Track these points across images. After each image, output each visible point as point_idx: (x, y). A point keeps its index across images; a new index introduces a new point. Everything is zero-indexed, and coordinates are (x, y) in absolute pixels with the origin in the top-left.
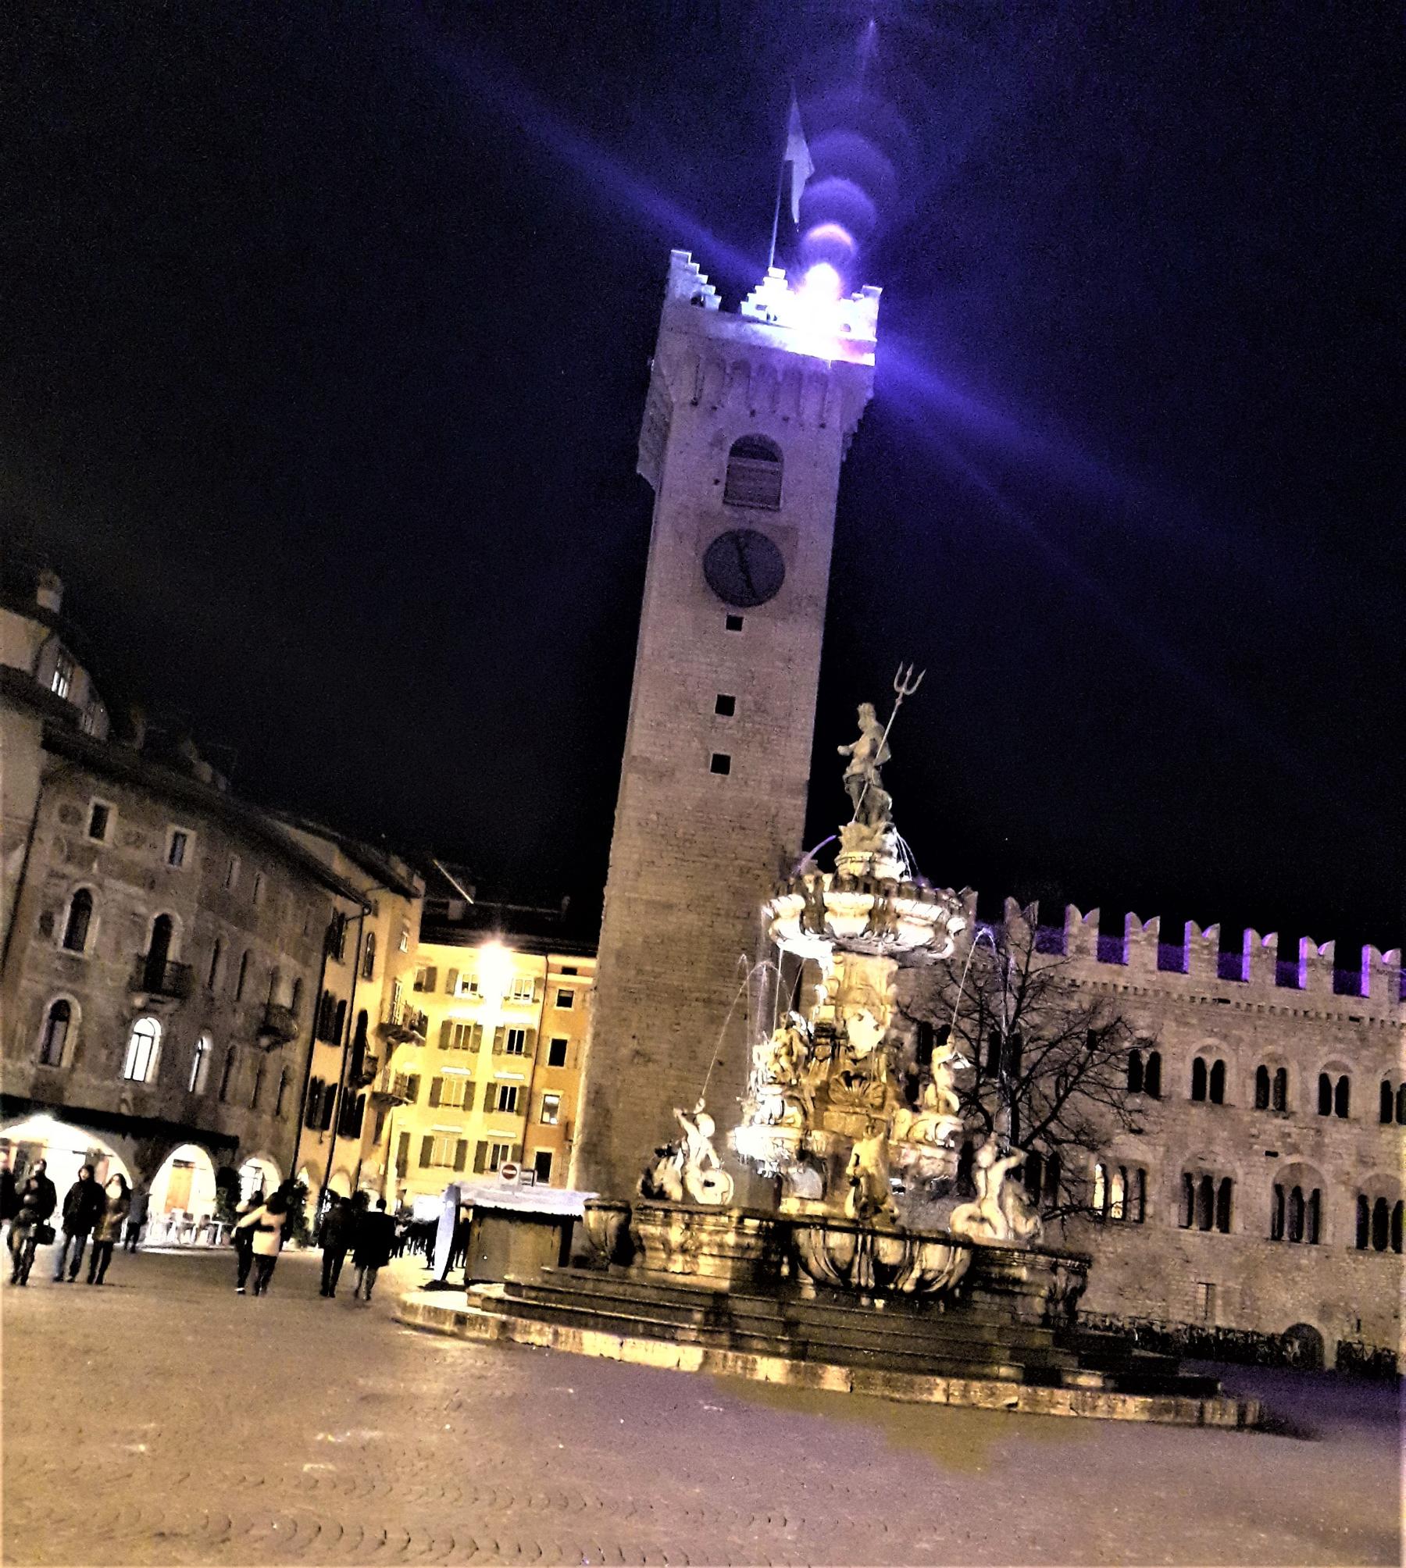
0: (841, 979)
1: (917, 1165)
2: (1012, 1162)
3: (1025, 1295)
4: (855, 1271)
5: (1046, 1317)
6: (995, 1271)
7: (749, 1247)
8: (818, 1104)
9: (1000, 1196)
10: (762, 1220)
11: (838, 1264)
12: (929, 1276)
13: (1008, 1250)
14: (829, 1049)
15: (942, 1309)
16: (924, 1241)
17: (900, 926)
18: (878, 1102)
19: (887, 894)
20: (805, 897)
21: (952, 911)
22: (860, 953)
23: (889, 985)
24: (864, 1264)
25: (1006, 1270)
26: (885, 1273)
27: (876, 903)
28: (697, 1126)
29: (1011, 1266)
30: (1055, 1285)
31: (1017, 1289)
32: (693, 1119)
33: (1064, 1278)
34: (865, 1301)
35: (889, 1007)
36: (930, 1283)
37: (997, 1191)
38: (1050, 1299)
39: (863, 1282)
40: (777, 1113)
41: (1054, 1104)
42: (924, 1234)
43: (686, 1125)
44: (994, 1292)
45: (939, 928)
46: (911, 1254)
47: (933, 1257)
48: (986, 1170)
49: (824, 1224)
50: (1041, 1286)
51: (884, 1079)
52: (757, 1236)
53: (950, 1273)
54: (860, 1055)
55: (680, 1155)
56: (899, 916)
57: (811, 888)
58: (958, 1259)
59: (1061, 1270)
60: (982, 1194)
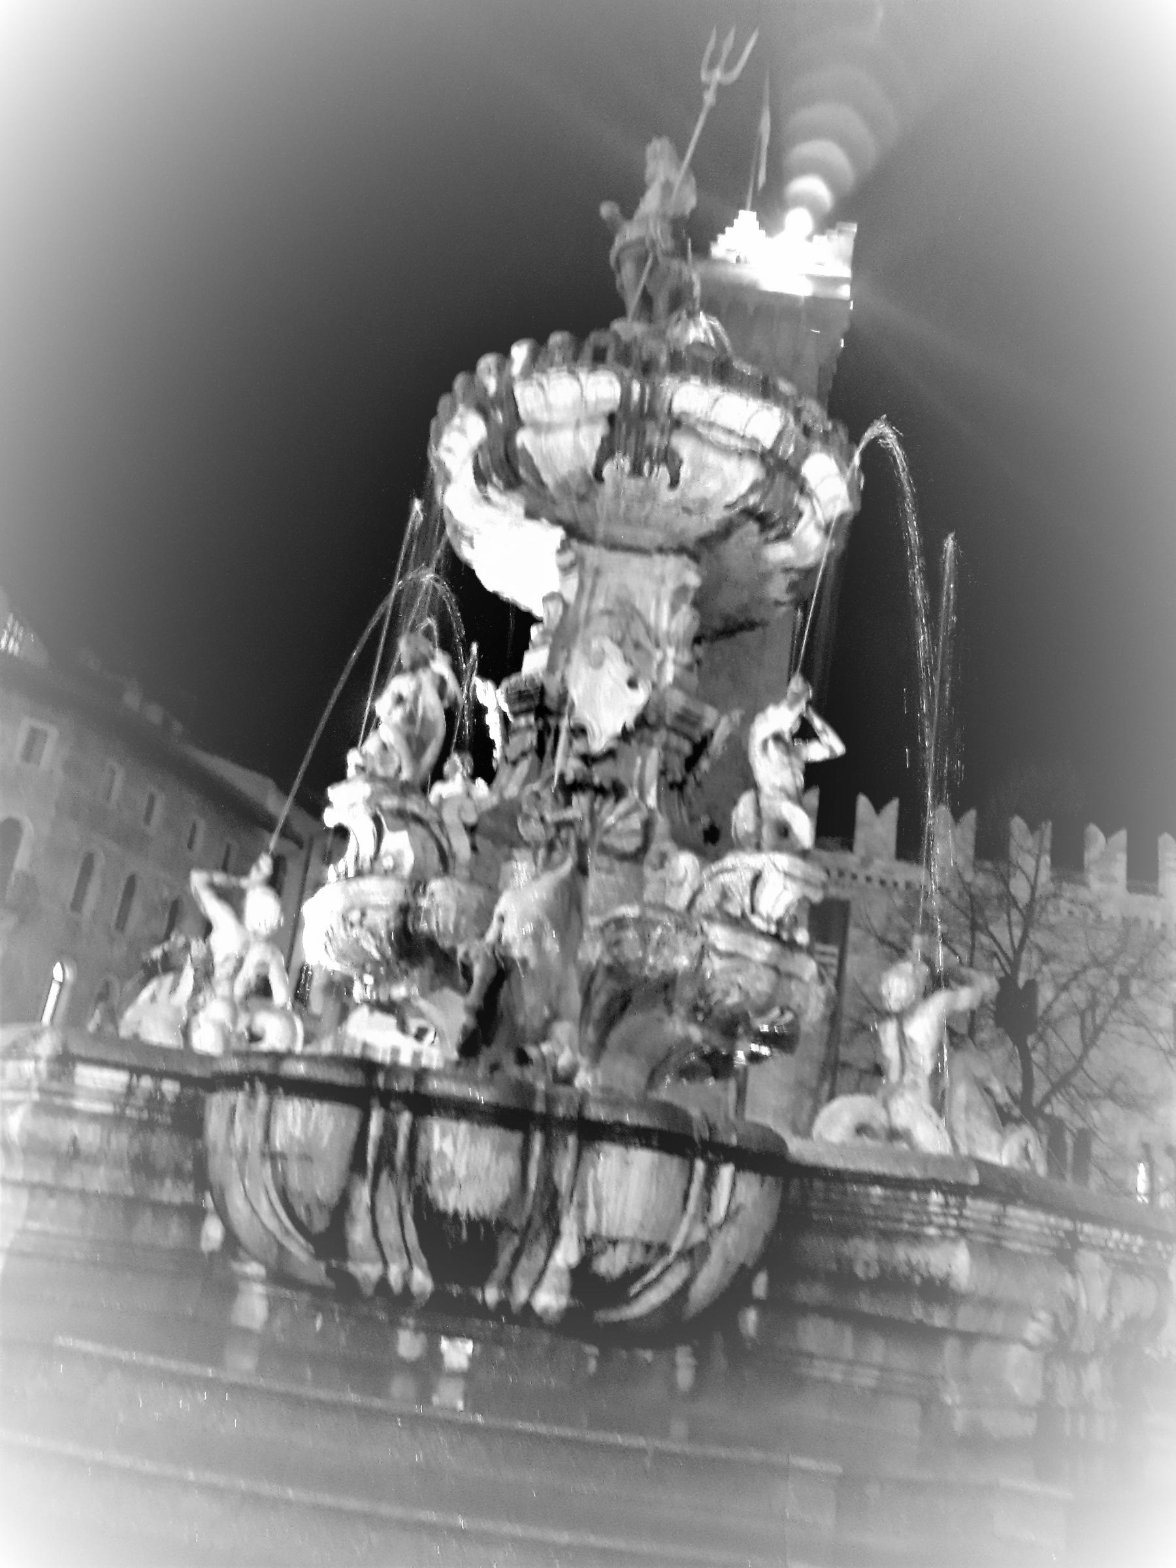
1: (696, 971)
2: (965, 998)
3: (969, 1339)
4: (359, 1234)
6: (865, 1253)
7: (75, 1154)
9: (936, 1076)
10: (136, 1071)
11: (301, 1212)
12: (611, 1264)
13: (904, 1184)
14: (531, 738)
15: (685, 1376)
16: (592, 1133)
17: (684, 446)
18: (631, 844)
19: (647, 369)
20: (484, 411)
21: (807, 431)
22: (613, 546)
23: (674, 609)
24: (387, 1212)
25: (902, 1253)
26: (464, 1250)
27: (626, 393)
28: (239, 912)
29: (916, 1238)
30: (1072, 1306)
31: (939, 1319)
32: (233, 899)
33: (1099, 1285)
34: (408, 1344)
35: (671, 652)
37: (927, 1065)
39: (395, 1274)
40: (368, 851)
42: (597, 1112)
43: (214, 908)
44: (864, 1324)
45: (781, 469)
46: (547, 1179)
48: (902, 1016)
49: (272, 1079)
51: (652, 800)
52: (117, 1119)
53: (695, 1254)
54: (598, 744)
57: (492, 385)
59: (1089, 1260)
60: (894, 1074)
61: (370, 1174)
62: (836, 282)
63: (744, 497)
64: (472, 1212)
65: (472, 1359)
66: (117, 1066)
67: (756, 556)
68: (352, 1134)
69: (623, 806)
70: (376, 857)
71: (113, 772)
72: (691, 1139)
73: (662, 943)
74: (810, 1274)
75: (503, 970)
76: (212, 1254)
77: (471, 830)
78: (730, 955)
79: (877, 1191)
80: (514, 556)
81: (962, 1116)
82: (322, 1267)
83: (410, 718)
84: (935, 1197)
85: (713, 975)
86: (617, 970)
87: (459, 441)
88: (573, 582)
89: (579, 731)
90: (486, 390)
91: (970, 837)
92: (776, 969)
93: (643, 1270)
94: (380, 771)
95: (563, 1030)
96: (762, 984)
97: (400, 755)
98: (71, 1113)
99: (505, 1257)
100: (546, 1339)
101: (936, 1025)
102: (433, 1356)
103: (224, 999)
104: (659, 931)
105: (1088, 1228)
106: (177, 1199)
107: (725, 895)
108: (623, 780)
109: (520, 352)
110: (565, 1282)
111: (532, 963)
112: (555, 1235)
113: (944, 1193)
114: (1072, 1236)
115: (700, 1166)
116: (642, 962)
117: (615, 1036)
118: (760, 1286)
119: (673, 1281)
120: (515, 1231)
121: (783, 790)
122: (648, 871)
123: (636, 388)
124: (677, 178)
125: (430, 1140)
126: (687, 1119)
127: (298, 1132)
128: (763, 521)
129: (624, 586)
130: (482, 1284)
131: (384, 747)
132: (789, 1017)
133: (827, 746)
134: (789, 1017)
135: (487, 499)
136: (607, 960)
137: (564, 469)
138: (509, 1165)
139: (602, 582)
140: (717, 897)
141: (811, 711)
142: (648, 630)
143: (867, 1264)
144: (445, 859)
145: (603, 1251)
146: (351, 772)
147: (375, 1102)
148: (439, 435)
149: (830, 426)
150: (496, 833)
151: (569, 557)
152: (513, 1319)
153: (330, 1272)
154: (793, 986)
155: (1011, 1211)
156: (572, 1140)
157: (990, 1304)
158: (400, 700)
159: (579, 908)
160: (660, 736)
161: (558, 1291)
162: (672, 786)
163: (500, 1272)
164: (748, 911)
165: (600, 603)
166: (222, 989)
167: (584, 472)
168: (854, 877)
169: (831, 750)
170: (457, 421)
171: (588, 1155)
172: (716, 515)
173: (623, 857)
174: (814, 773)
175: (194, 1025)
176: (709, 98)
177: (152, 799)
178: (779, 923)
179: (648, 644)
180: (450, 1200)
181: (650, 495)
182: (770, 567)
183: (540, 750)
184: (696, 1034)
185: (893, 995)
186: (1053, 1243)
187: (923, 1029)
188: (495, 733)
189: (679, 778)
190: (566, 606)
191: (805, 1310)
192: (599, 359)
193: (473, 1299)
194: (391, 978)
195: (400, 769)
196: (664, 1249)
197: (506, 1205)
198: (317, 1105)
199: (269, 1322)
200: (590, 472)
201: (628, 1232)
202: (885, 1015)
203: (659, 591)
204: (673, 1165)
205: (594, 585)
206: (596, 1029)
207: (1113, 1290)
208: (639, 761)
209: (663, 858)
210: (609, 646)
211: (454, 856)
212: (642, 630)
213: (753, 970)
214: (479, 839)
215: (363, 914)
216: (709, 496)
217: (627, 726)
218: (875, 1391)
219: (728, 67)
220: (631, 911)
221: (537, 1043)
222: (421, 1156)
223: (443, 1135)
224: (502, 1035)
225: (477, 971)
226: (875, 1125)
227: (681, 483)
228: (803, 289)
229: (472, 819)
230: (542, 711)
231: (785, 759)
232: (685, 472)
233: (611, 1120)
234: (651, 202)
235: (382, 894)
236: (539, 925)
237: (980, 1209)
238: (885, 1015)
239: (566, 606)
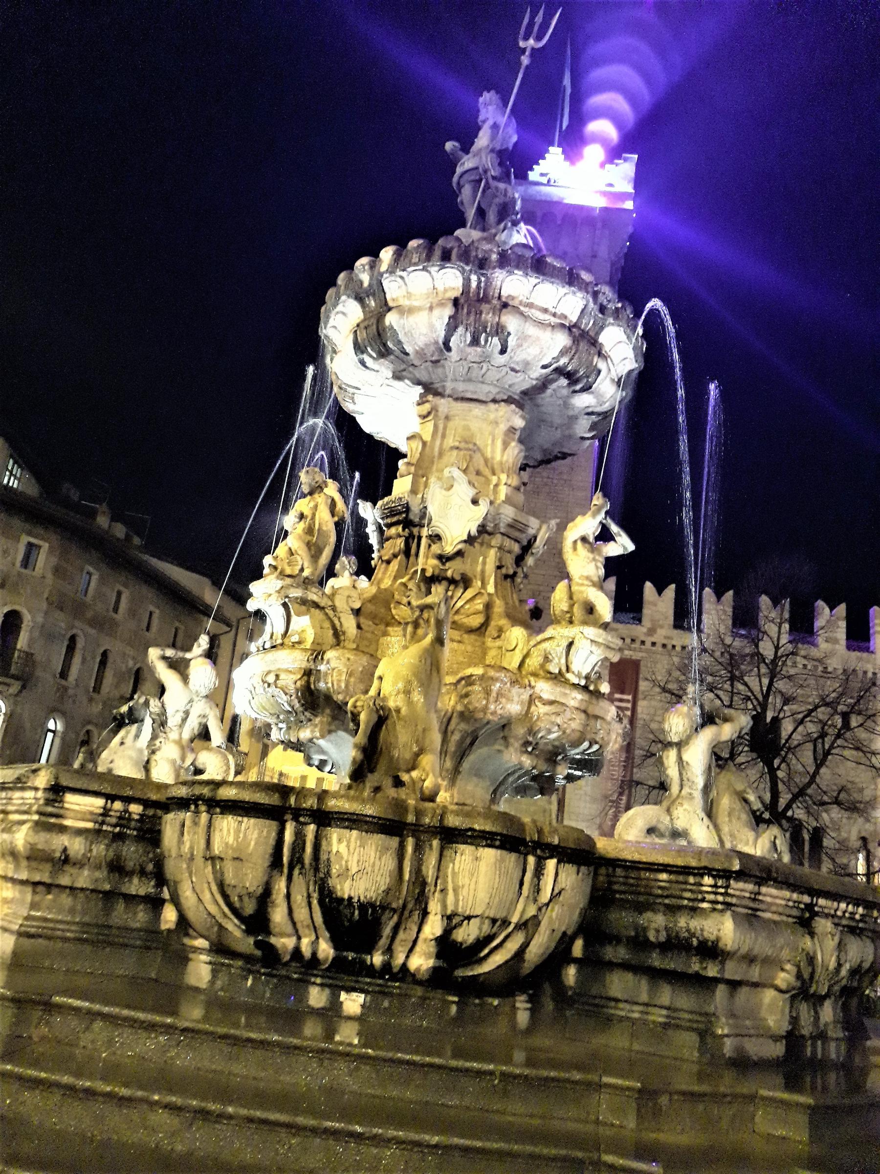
0: (427, 437)
2: (727, 731)
3: (734, 985)
4: (278, 915)
5: (793, 1039)
6: (656, 923)
7: (65, 860)
8: (365, 623)
9: (707, 789)
10: (111, 798)
12: (467, 934)
13: (686, 870)
14: (400, 543)
15: (523, 1017)
16: (451, 837)
17: (511, 322)
18: (476, 621)
19: (482, 264)
20: (360, 299)
21: (602, 309)
23: (506, 445)
24: (299, 898)
25: (683, 922)
27: (467, 282)
28: (185, 678)
29: (694, 910)
30: (811, 960)
31: (712, 971)
32: (179, 667)
33: (831, 944)
34: (317, 997)
35: (504, 477)
36: (474, 952)
37: (700, 782)
38: (803, 992)
40: (280, 628)
41: (812, 770)
42: (453, 821)
44: (656, 975)
45: (584, 338)
46: (418, 871)
47: (475, 880)
49: (213, 802)
50: (772, 963)
51: (491, 589)
53: (529, 926)
54: (449, 549)
55: (148, 721)
56: (505, 305)
58: (546, 895)
59: (823, 925)
60: (675, 789)
61: (286, 870)
62: (622, 196)
63: (556, 359)
64: (362, 898)
65: (363, 1006)
66: (96, 794)
67: (566, 405)
68: (272, 841)
69: (469, 593)
70: (285, 635)
71: (89, 574)
72: (525, 839)
73: (499, 694)
74: (615, 939)
75: (382, 718)
76: (169, 931)
77: (357, 612)
78: (551, 703)
79: (664, 876)
80: (385, 408)
81: (727, 819)
82: (251, 940)
83: (310, 531)
84: (708, 880)
85: (538, 718)
86: (466, 716)
87: (341, 320)
88: (430, 426)
89: (436, 538)
90: (361, 283)
91: (730, 611)
92: (585, 712)
93: (490, 938)
94: (288, 571)
95: (428, 761)
96: (576, 724)
97: (303, 558)
98: (63, 829)
99: (387, 931)
100: (419, 991)
101: (706, 751)
102: (335, 1006)
103: (175, 742)
104: (498, 685)
105: (822, 902)
106: (142, 892)
107: (547, 659)
108: (470, 574)
109: (387, 254)
110: (432, 948)
111: (404, 711)
112: (425, 913)
113: (714, 877)
114: (810, 907)
115: (531, 860)
116: (485, 709)
117: (466, 765)
118: (578, 948)
119: (513, 946)
120: (394, 911)
121: (588, 578)
122: (489, 642)
123: (474, 278)
124: (502, 120)
125: (330, 844)
126: (521, 826)
127: (231, 840)
128: (571, 377)
129: (467, 428)
130: (370, 952)
131: (291, 553)
132: (595, 747)
133: (622, 544)
134: (595, 747)
135: (363, 363)
136: (459, 708)
137: (421, 341)
138: (389, 863)
139: (451, 424)
140: (541, 659)
141: (609, 520)
142: (486, 461)
143: (657, 931)
144: (338, 635)
145: (460, 924)
146: (266, 571)
147: (288, 817)
148: (328, 317)
149: (620, 305)
150: (375, 615)
151: (427, 407)
152: (394, 977)
153: (258, 944)
154: (599, 721)
155: (764, 890)
156: (436, 843)
157: (750, 959)
158: (302, 516)
159: (438, 671)
160: (497, 540)
161: (428, 956)
162: (506, 577)
163: (383, 942)
164: (564, 669)
165: (450, 442)
166: (173, 735)
167: (437, 343)
168: (643, 643)
169: (625, 548)
170: (340, 308)
171: (448, 853)
172: (537, 373)
173: (471, 631)
174: (612, 565)
175: (153, 763)
176: (525, 60)
177: (119, 594)
178: (587, 677)
179: (486, 472)
180: (345, 889)
181: (486, 359)
182: (576, 412)
183: (407, 552)
184: (527, 762)
185: (674, 731)
186: (795, 912)
187: (697, 755)
188: (373, 540)
189: (511, 572)
190: (424, 444)
191: (611, 966)
192: (446, 257)
193: (364, 962)
194: (300, 724)
195: (302, 570)
196: (505, 923)
197: (387, 892)
198: (245, 819)
199: (212, 982)
200: (441, 341)
201: (478, 912)
202: (668, 745)
203: (495, 432)
204: (511, 859)
205: (445, 428)
206: (452, 759)
207: (841, 946)
208: (481, 558)
209: (501, 630)
210: (457, 473)
211: (344, 633)
212: (482, 462)
213: (568, 714)
214: (362, 620)
215: (277, 676)
216: (529, 359)
217: (472, 534)
218: (665, 1026)
219: (539, 38)
220: (478, 671)
221: (408, 771)
222: (323, 857)
223: (340, 841)
224: (382, 766)
225: (363, 717)
226: (662, 827)
227: (509, 350)
228: (599, 202)
229: (357, 605)
230: (407, 523)
231: (591, 556)
232: (512, 342)
233: (464, 826)
234: (483, 140)
235: (291, 662)
236: (409, 682)
237: (741, 888)
238: (668, 745)
239: (424, 444)
